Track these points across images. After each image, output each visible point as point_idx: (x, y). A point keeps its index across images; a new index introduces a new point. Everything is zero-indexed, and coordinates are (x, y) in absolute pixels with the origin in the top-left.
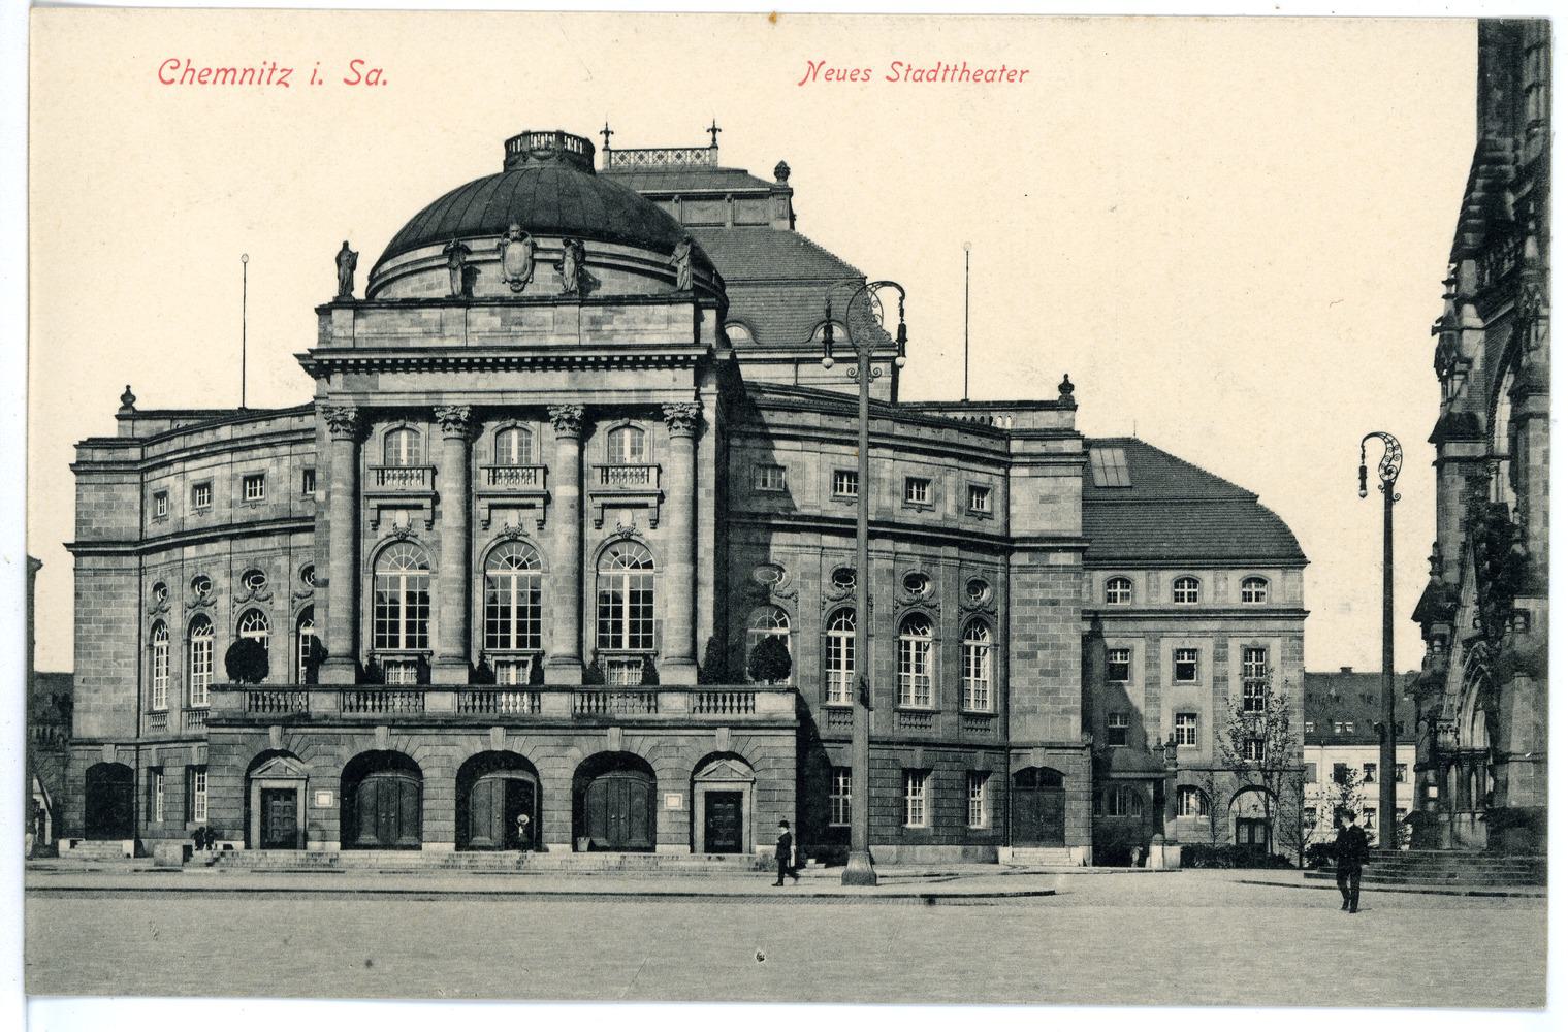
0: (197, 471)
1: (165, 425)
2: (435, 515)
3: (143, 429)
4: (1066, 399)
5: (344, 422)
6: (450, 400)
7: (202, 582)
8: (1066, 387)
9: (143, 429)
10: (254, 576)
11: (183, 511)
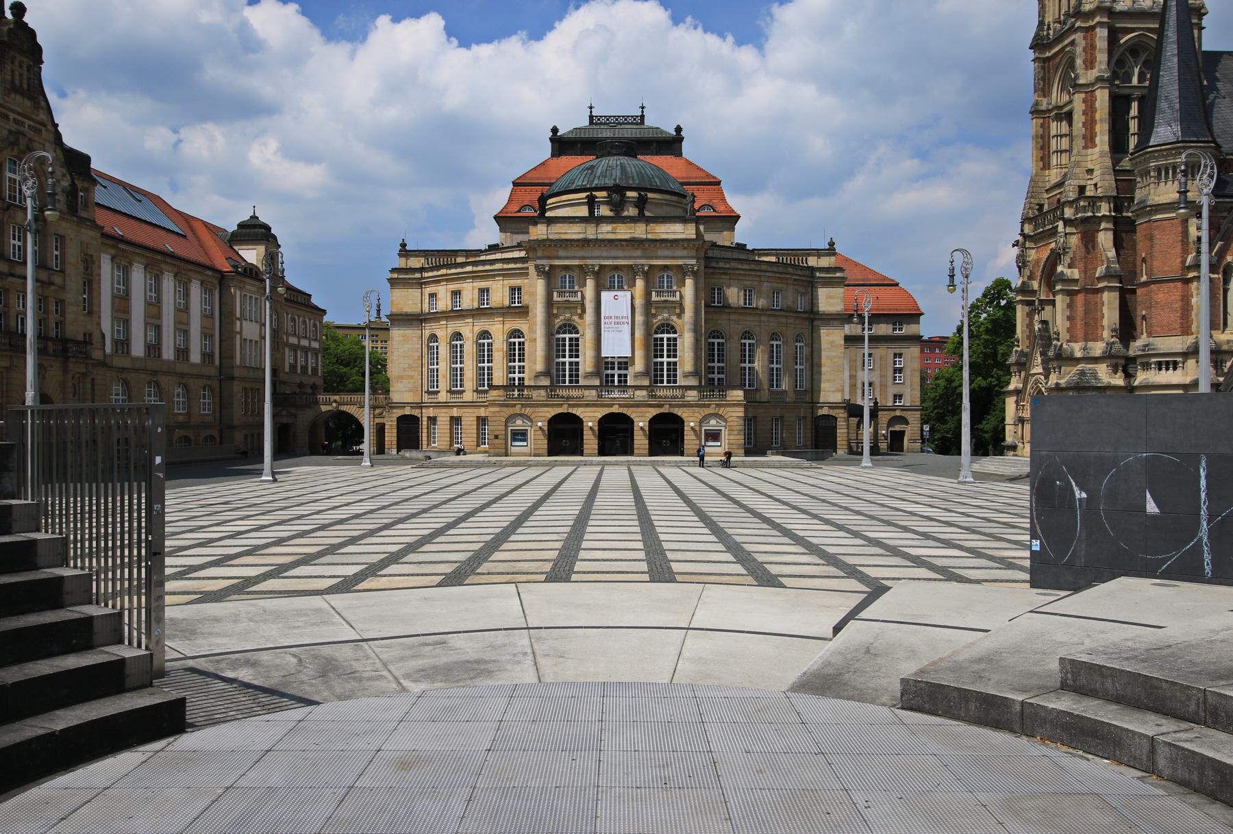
0: (454, 286)
2: (584, 311)
3: (416, 263)
5: (544, 272)
6: (589, 262)
7: (458, 336)
8: (832, 244)
9: (416, 263)
10: (485, 334)
11: (444, 303)
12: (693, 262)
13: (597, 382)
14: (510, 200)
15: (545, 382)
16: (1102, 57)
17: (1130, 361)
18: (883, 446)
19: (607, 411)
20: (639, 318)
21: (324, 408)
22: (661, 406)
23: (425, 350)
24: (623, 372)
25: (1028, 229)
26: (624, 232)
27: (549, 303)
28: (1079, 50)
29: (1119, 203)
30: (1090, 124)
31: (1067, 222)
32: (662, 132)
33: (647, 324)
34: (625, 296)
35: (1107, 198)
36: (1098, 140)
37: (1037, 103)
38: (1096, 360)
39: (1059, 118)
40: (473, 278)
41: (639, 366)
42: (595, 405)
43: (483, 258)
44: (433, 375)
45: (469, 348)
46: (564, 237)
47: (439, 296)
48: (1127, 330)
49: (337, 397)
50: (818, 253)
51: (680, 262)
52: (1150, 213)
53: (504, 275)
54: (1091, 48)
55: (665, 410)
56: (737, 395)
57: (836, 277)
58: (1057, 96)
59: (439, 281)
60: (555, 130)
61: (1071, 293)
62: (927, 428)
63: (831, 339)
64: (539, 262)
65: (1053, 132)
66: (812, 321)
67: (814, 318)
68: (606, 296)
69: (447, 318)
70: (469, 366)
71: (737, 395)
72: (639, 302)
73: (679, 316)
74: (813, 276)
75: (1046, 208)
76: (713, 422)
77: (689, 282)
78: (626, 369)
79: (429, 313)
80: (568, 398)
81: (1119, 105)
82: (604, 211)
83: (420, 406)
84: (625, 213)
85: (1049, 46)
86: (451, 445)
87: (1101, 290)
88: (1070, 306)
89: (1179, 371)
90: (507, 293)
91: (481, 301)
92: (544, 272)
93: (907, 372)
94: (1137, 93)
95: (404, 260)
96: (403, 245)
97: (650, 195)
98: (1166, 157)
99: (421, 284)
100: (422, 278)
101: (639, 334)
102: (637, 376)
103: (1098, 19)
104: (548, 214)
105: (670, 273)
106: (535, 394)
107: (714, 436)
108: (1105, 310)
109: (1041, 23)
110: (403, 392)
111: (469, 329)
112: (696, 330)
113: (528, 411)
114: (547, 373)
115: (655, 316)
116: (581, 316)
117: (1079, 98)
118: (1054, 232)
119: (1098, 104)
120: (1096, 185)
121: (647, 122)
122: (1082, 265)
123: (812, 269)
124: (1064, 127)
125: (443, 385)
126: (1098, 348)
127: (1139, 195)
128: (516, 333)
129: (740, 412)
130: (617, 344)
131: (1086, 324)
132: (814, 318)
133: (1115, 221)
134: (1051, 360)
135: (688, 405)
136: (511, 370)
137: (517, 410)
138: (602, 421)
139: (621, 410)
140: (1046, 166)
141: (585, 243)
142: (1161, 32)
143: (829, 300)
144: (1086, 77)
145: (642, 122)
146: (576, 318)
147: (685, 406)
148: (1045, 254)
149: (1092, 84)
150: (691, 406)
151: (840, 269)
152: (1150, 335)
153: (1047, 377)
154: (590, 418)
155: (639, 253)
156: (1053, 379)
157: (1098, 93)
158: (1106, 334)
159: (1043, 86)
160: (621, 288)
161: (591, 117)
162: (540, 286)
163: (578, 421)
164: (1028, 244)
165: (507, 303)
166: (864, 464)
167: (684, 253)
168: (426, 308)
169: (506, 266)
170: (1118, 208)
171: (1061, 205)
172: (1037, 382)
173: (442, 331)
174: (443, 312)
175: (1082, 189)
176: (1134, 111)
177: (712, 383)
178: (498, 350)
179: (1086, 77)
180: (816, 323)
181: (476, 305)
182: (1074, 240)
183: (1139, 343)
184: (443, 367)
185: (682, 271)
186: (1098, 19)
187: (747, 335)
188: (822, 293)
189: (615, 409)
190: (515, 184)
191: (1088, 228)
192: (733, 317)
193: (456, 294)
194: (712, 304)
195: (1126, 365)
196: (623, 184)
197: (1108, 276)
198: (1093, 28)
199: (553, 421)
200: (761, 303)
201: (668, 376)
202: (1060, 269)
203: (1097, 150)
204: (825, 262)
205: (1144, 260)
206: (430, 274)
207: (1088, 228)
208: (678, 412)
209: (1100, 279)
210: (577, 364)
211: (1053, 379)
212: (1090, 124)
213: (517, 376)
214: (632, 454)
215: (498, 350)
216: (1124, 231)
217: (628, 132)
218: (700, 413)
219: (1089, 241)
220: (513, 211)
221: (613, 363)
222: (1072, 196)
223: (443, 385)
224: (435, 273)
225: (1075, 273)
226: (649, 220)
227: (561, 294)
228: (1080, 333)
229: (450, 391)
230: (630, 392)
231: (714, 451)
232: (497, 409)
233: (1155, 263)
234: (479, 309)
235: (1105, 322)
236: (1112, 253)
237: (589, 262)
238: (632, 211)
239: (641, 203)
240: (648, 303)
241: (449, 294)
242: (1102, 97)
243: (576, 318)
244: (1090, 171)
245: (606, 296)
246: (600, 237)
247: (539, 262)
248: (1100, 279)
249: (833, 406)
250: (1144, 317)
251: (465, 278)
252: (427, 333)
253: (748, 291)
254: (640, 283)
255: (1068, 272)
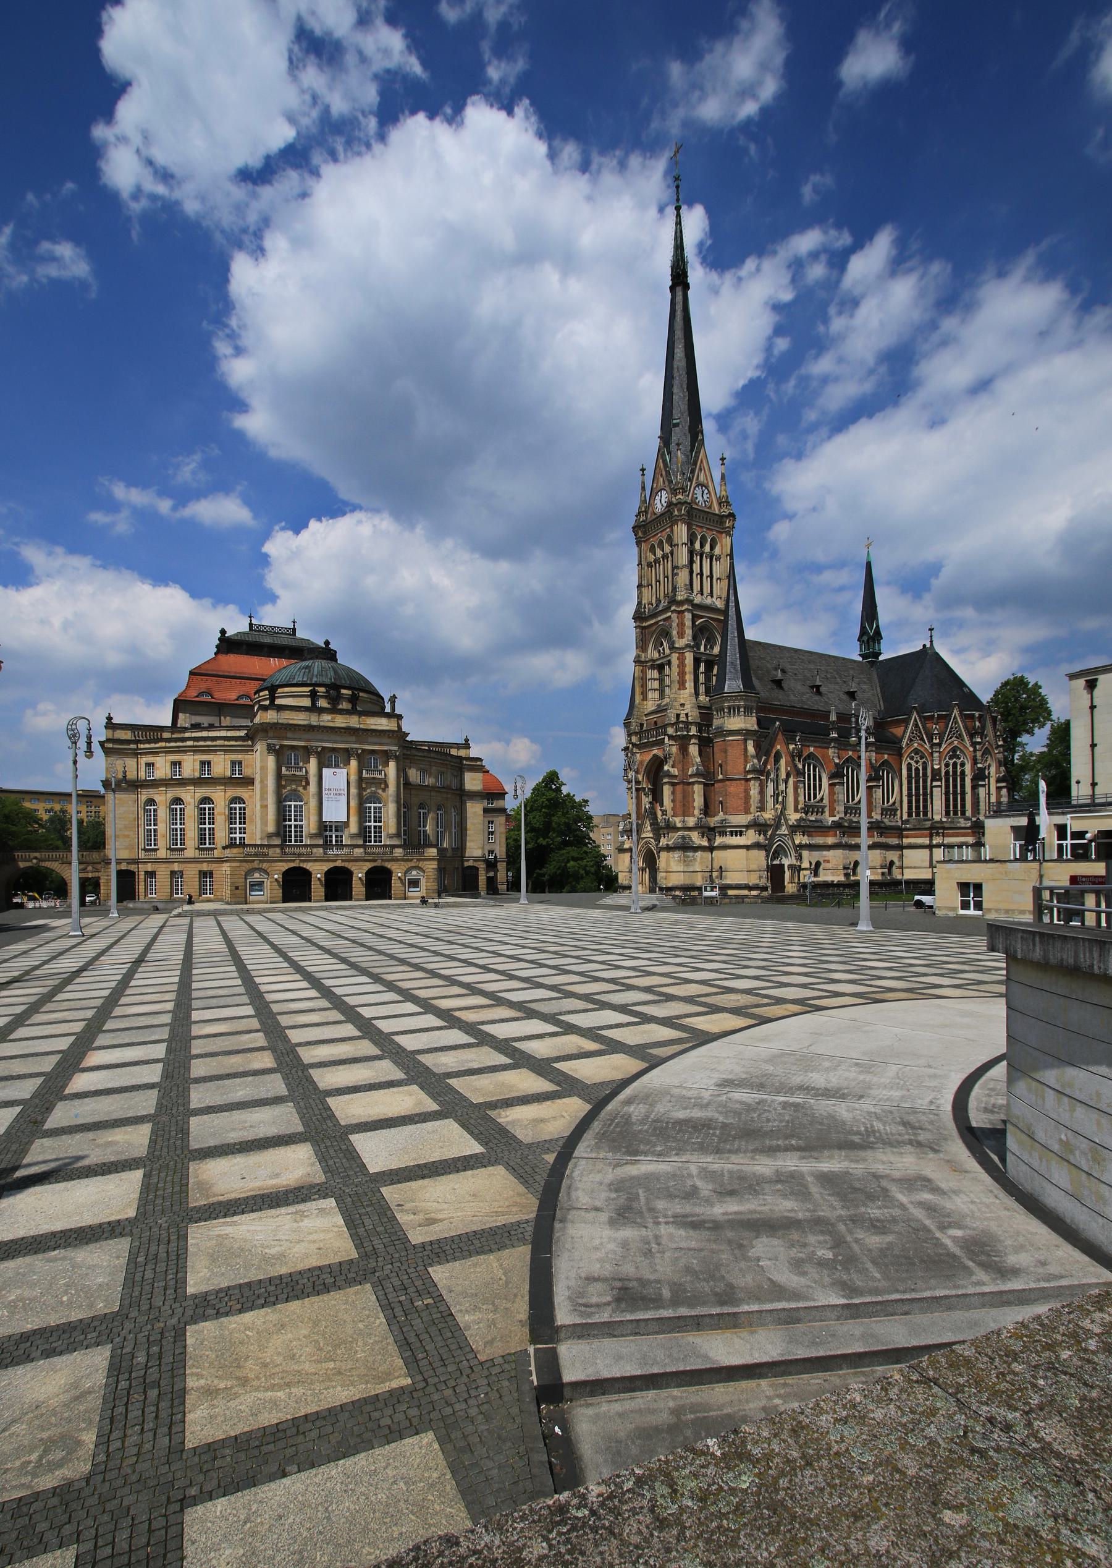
1: (140, 736)
2: (308, 783)
4: (466, 745)
5: (275, 750)
6: (313, 744)
7: (178, 800)
8: (467, 740)
9: (127, 735)
10: (206, 800)
12: (396, 748)
13: (321, 842)
14: (188, 686)
15: (278, 841)
16: (689, 632)
17: (712, 830)
18: (502, 887)
19: (332, 865)
20: (354, 791)
21: (22, 865)
22: (374, 861)
23: (141, 812)
24: (339, 834)
25: (634, 739)
26: (341, 721)
27: (279, 776)
28: (674, 625)
29: (700, 726)
30: (682, 674)
31: (670, 737)
32: (313, 643)
33: (360, 796)
34: (342, 773)
35: (695, 724)
36: (687, 685)
37: (638, 656)
38: (690, 829)
39: (652, 667)
40: (194, 751)
41: (354, 828)
42: (321, 861)
43: (187, 735)
44: (151, 836)
45: (191, 812)
46: (291, 722)
47: (157, 765)
48: (707, 810)
49: (37, 855)
50: (458, 746)
51: (385, 748)
52: (725, 736)
53: (225, 751)
54: (681, 625)
55: (378, 863)
56: (433, 852)
57: (477, 765)
58: (652, 653)
59: (157, 753)
60: (223, 632)
61: (673, 784)
62: (510, 874)
63: (474, 810)
64: (270, 741)
65: (649, 677)
66: (461, 796)
67: (463, 795)
68: (325, 770)
69: (166, 785)
70: (191, 827)
71: (433, 852)
72: (353, 778)
73: (384, 790)
74: (462, 764)
75: (645, 728)
76: (414, 873)
77: (392, 764)
78: (342, 831)
79: (146, 780)
80: (300, 855)
81: (697, 662)
82: (322, 703)
83: (136, 862)
84: (340, 707)
85: (646, 619)
86: (172, 895)
87: (693, 783)
88: (673, 793)
89: (743, 837)
90: (229, 766)
91: (202, 772)
92: (275, 750)
93: (498, 834)
94: (704, 658)
95: (110, 731)
96: (109, 718)
97: (361, 694)
98: (734, 701)
99: (136, 754)
100: (138, 749)
101: (353, 803)
102: (352, 836)
103: (686, 607)
104: (278, 702)
105: (377, 756)
106: (271, 852)
107: (414, 883)
108: (696, 796)
109: (639, 603)
110: (120, 848)
111: (190, 797)
112: (398, 802)
113: (265, 865)
114: (277, 834)
115: (365, 789)
116: (305, 788)
117: (674, 658)
118: (661, 742)
119: (687, 662)
120: (687, 715)
121: (299, 634)
122: (680, 766)
123: (461, 758)
124: (655, 674)
125: (163, 843)
126: (691, 821)
127: (716, 723)
128: (238, 800)
129: (434, 865)
130: (336, 810)
131: (684, 805)
132: (463, 795)
133: (700, 738)
134: (662, 828)
135: (396, 860)
136: (232, 831)
137: (256, 865)
138: (328, 873)
139: (343, 865)
140: (645, 698)
141: (310, 728)
142: (725, 623)
143: (473, 782)
144: (680, 643)
145: (294, 633)
146: (300, 789)
147: (393, 860)
148: (648, 757)
149: (683, 649)
150: (398, 860)
151: (480, 760)
152: (725, 813)
153: (658, 840)
154: (318, 871)
155: (353, 739)
156: (663, 842)
157: (687, 654)
158: (696, 812)
159: (642, 645)
160: (337, 766)
161: (251, 625)
162: (271, 761)
163: (307, 874)
164: (635, 750)
165: (228, 774)
166: (522, 901)
167: (389, 741)
168: (142, 775)
169: (226, 743)
170: (700, 731)
171: (665, 726)
172: (646, 843)
173: (163, 797)
174: (161, 780)
175: (678, 716)
176: (702, 669)
177: (412, 840)
178: (219, 814)
179: (680, 643)
180: (465, 798)
181: (197, 775)
182: (674, 749)
183: (717, 818)
184: (163, 827)
185: (387, 756)
186: (686, 607)
187: (422, 806)
188: (468, 776)
189: (339, 864)
190: (191, 673)
191: (683, 742)
192: (413, 792)
193: (176, 764)
194: (405, 784)
195: (709, 832)
196: (338, 683)
197: (697, 774)
198: (683, 612)
199: (287, 874)
200: (430, 781)
201: (296, 836)
202: (666, 768)
203: (687, 691)
204: (462, 753)
205: (721, 765)
206: (147, 746)
207: (683, 742)
208: (388, 865)
209: (691, 776)
210: (301, 827)
211: (663, 842)
212: (682, 674)
213: (238, 836)
214: (351, 899)
215: (219, 814)
216: (705, 743)
217: (285, 641)
218: (405, 866)
219: (684, 750)
220: (192, 695)
221: (331, 826)
222: (673, 720)
223: (163, 843)
224: (153, 745)
225: (675, 771)
226: (361, 714)
227: (288, 769)
228: (679, 811)
229: (170, 849)
230: (346, 850)
231: (416, 894)
232: (238, 864)
233: (729, 768)
234: (200, 778)
235: (696, 804)
236: (698, 760)
237: (313, 744)
238: (345, 705)
239: (353, 700)
240: (360, 779)
241: (168, 765)
242: (689, 657)
243: (300, 789)
244: (683, 705)
245: (325, 770)
246: (322, 724)
247: (270, 741)
248: (691, 776)
249: (476, 859)
250: (721, 802)
251: (185, 752)
252: (143, 797)
253: (423, 772)
254: (354, 763)
255: (671, 770)
